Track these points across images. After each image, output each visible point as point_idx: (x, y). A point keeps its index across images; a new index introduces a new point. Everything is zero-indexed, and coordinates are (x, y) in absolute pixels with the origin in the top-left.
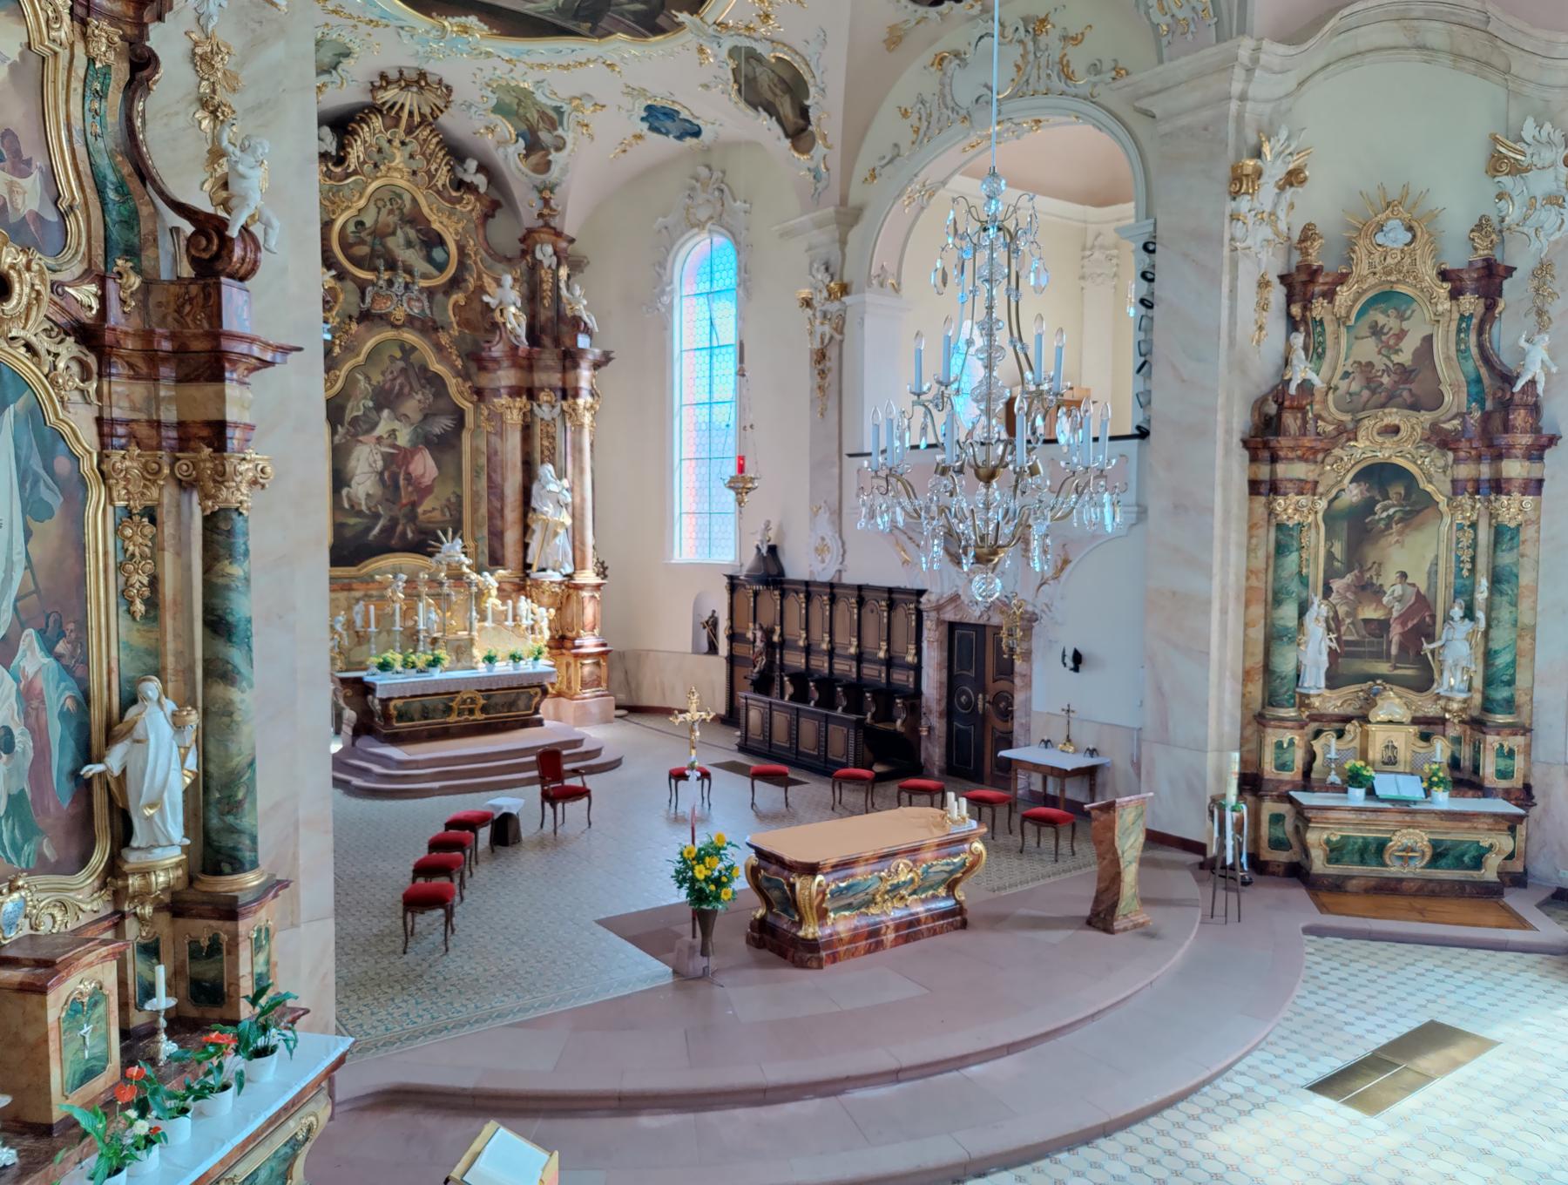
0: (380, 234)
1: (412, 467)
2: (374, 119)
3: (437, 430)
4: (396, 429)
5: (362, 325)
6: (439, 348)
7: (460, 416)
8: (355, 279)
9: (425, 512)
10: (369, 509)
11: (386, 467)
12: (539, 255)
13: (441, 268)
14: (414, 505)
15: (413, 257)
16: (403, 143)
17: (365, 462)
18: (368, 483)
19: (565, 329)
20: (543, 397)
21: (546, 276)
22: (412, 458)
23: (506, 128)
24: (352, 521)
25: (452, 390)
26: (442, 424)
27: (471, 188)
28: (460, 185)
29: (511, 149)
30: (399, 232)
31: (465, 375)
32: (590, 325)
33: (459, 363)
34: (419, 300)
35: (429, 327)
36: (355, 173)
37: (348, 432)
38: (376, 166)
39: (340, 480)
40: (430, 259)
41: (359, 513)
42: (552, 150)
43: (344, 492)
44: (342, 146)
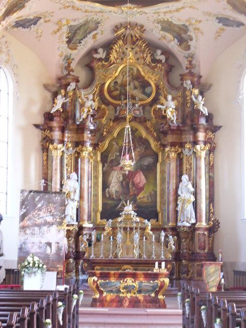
0: (124, 85)
1: (135, 179)
2: (119, 42)
3: (146, 163)
4: (128, 163)
5: (115, 123)
6: (147, 129)
7: (156, 156)
8: (112, 104)
9: (140, 198)
10: (117, 197)
11: (124, 180)
12: (185, 85)
13: (149, 95)
14: (136, 195)
15: (138, 93)
16: (132, 49)
17: (115, 179)
18: (116, 186)
19: (196, 116)
20: (188, 146)
21: (188, 93)
22: (135, 175)
23: (169, 36)
24: (110, 202)
25: (153, 146)
26: (148, 161)
27: (160, 61)
28: (154, 60)
29: (173, 43)
30: (131, 84)
31: (158, 139)
32: (204, 113)
33: (155, 134)
34: (138, 110)
35: (142, 121)
36: (114, 63)
37: (109, 166)
38: (122, 59)
39: (105, 185)
40: (144, 93)
41: (113, 199)
42: (189, 41)
43: (107, 190)
44: (108, 55)
